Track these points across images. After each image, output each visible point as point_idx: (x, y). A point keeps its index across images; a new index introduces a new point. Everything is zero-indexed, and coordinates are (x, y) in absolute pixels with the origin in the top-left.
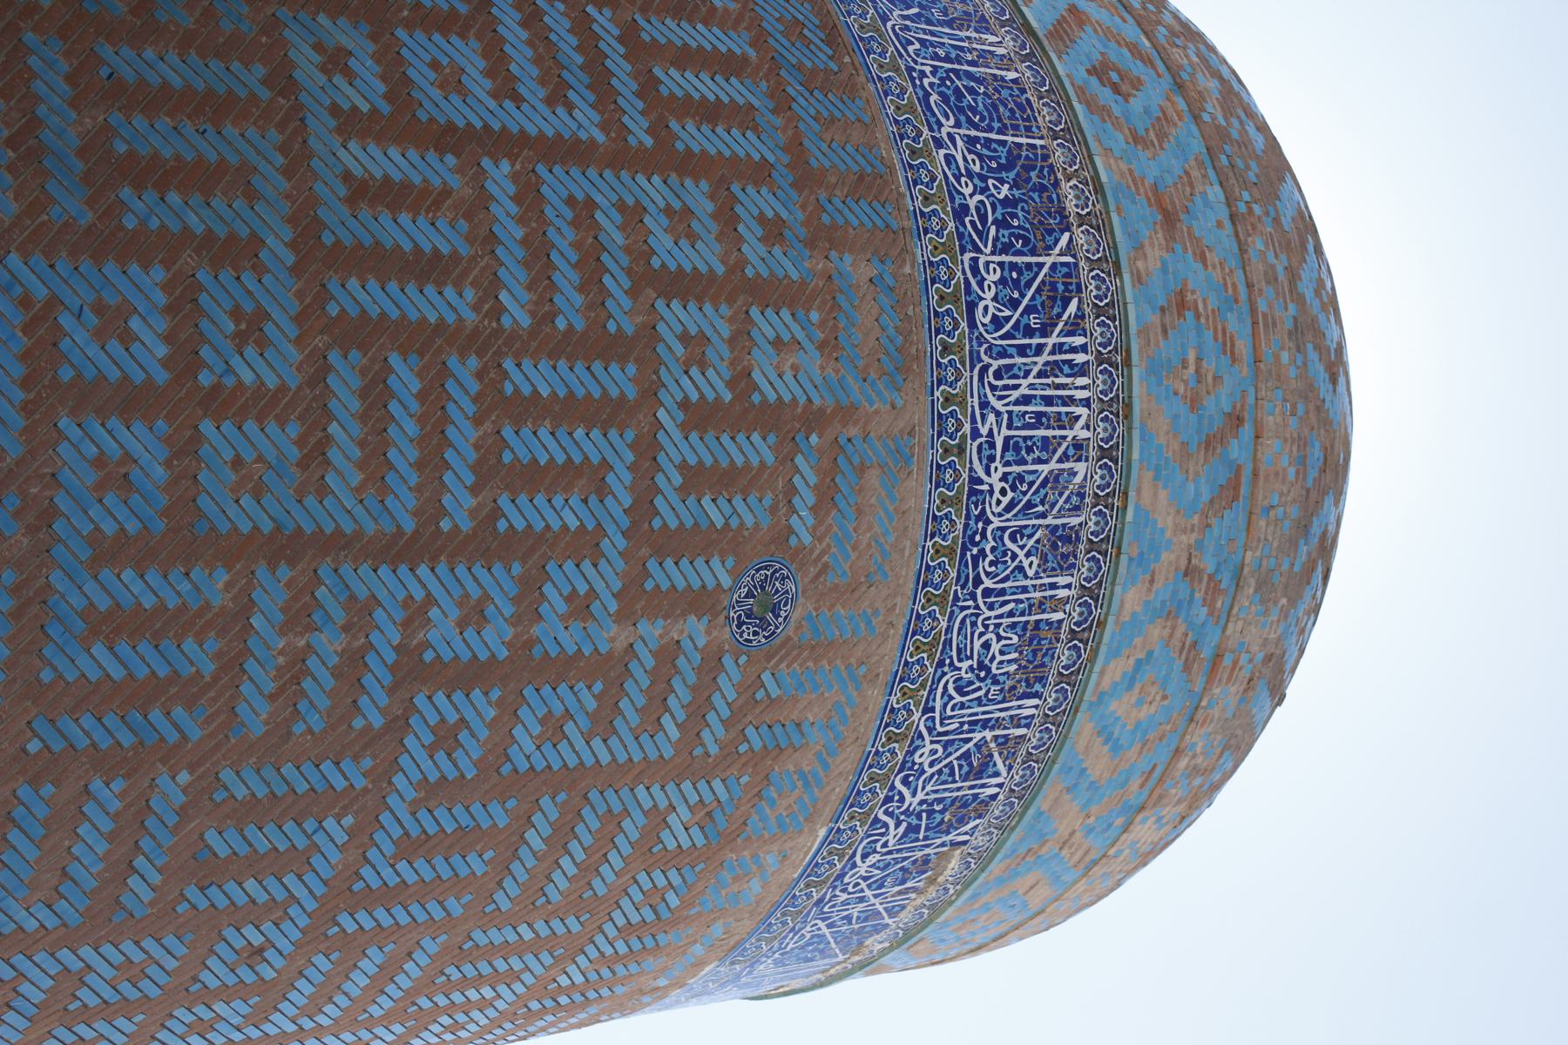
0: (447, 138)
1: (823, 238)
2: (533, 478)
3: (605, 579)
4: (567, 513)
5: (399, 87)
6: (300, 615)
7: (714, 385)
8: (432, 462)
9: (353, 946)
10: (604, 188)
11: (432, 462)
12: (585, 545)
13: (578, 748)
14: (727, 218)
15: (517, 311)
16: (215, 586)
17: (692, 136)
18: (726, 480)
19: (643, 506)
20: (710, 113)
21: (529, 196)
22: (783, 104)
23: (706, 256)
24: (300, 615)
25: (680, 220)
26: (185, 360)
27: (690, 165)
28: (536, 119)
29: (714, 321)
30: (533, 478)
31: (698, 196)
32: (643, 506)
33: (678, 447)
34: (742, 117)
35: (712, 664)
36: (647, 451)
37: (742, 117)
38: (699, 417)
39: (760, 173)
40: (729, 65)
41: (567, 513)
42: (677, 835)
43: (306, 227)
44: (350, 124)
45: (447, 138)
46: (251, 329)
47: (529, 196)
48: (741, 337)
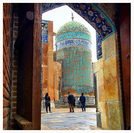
0: (70, 62)
1: (71, 50)
2: (78, 60)
3: (80, 58)
4: (79, 59)
5: (69, 63)
6: (81, 66)
7: (75, 54)
8: (77, 63)
9: (89, 63)
10: (71, 58)
11: (77, 63)
12: (80, 58)
13: (84, 58)
14: (71, 54)
15: (74, 61)
16: (81, 69)
17: (69, 54)
18: (78, 54)
19: (79, 57)
20: (68, 54)
21: (71, 60)
22: (67, 51)
23: (72, 54)
24: (81, 66)
25: (71, 55)
26: (76, 70)
27: (70, 55)
28: (69, 59)
29: (74, 54)
30: (78, 60)
31: (71, 55)
32: (79, 57)
33: (77, 56)
34: (68, 52)
35: (83, 54)
36: (77, 57)
37: (68, 52)
38: (76, 55)
39: (70, 52)
40: (67, 53)
41: (79, 59)
42: (87, 54)
43: (72, 66)
44: (70, 65)
45: (70, 62)
46: (75, 68)
47: (71, 60)
48: (74, 53)
